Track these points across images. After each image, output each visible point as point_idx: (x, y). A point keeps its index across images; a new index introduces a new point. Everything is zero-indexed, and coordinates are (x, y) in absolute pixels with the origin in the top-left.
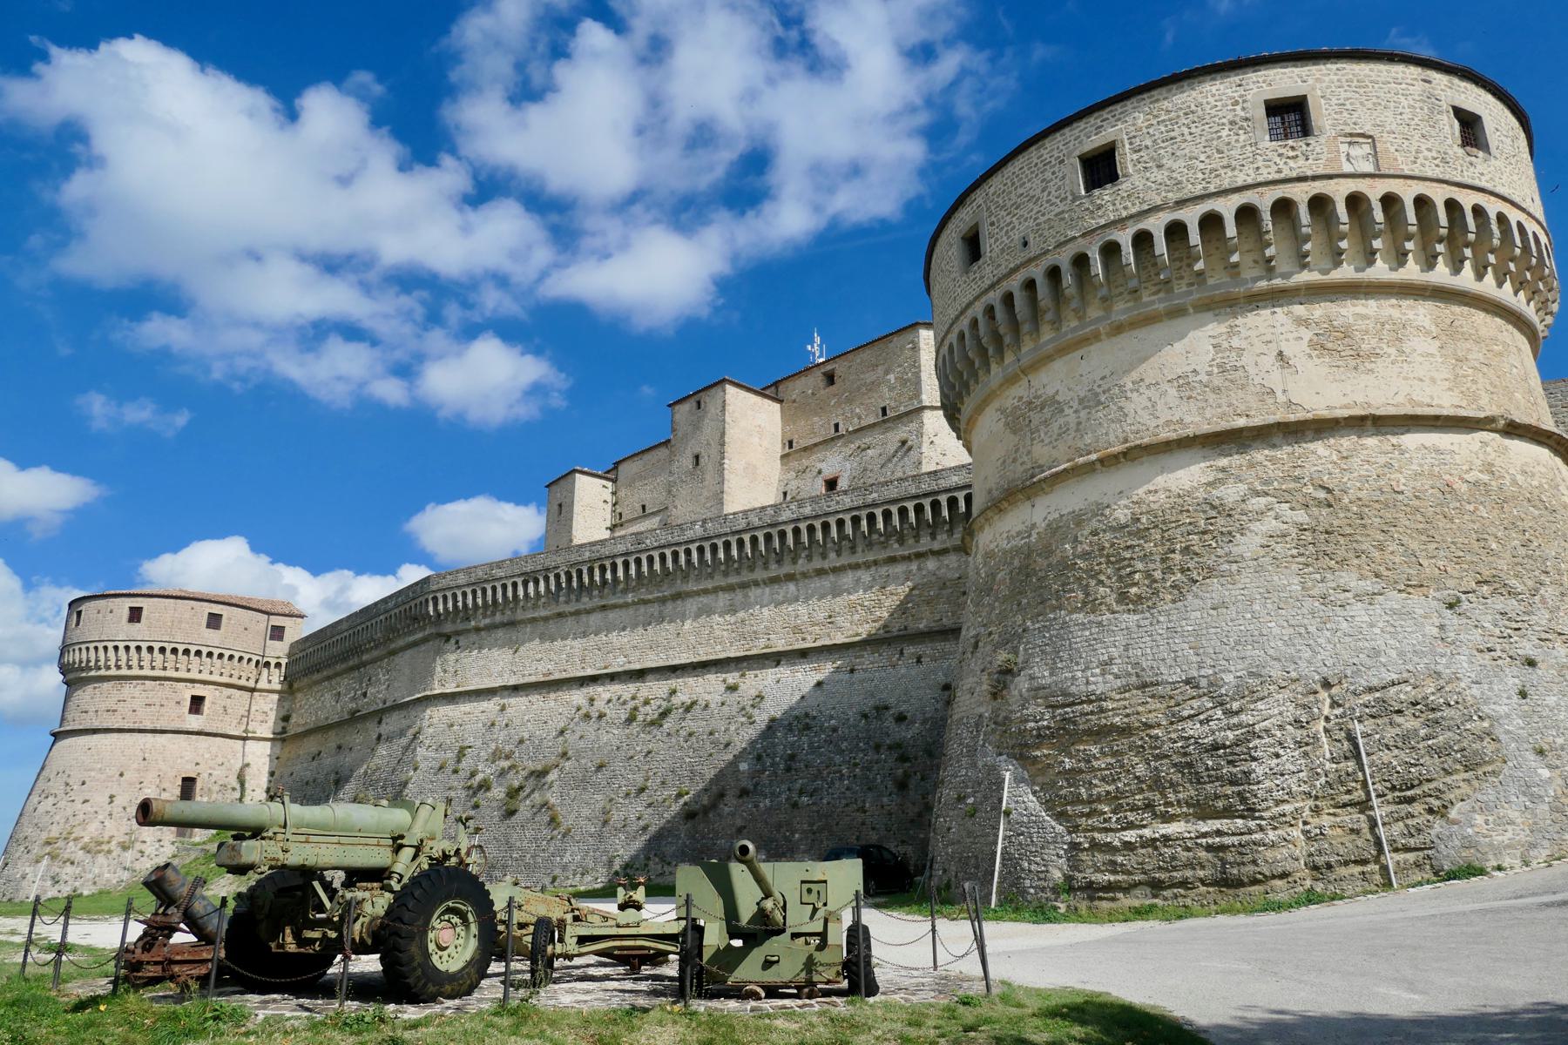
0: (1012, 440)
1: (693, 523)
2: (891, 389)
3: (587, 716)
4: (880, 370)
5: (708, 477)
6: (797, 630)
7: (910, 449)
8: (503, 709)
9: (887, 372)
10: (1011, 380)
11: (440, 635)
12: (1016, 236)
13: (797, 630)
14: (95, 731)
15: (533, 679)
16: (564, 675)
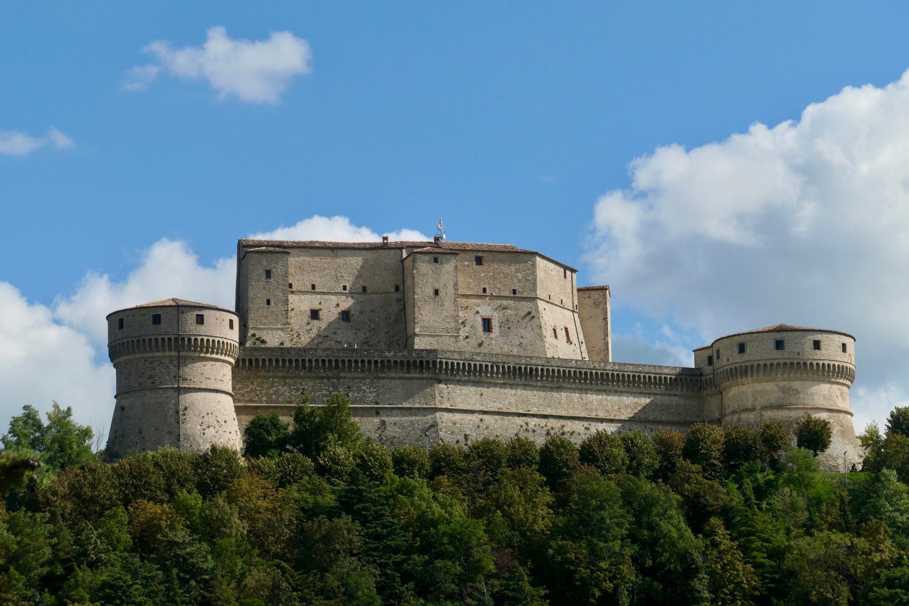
0: (782, 395)
1: (572, 360)
2: (519, 281)
3: (527, 430)
4: (513, 268)
5: (446, 304)
6: (608, 411)
7: (533, 317)
8: (481, 420)
9: (517, 271)
10: (784, 380)
11: (436, 379)
12: (797, 350)
13: (608, 411)
14: (217, 391)
15: (492, 410)
16: (508, 411)
